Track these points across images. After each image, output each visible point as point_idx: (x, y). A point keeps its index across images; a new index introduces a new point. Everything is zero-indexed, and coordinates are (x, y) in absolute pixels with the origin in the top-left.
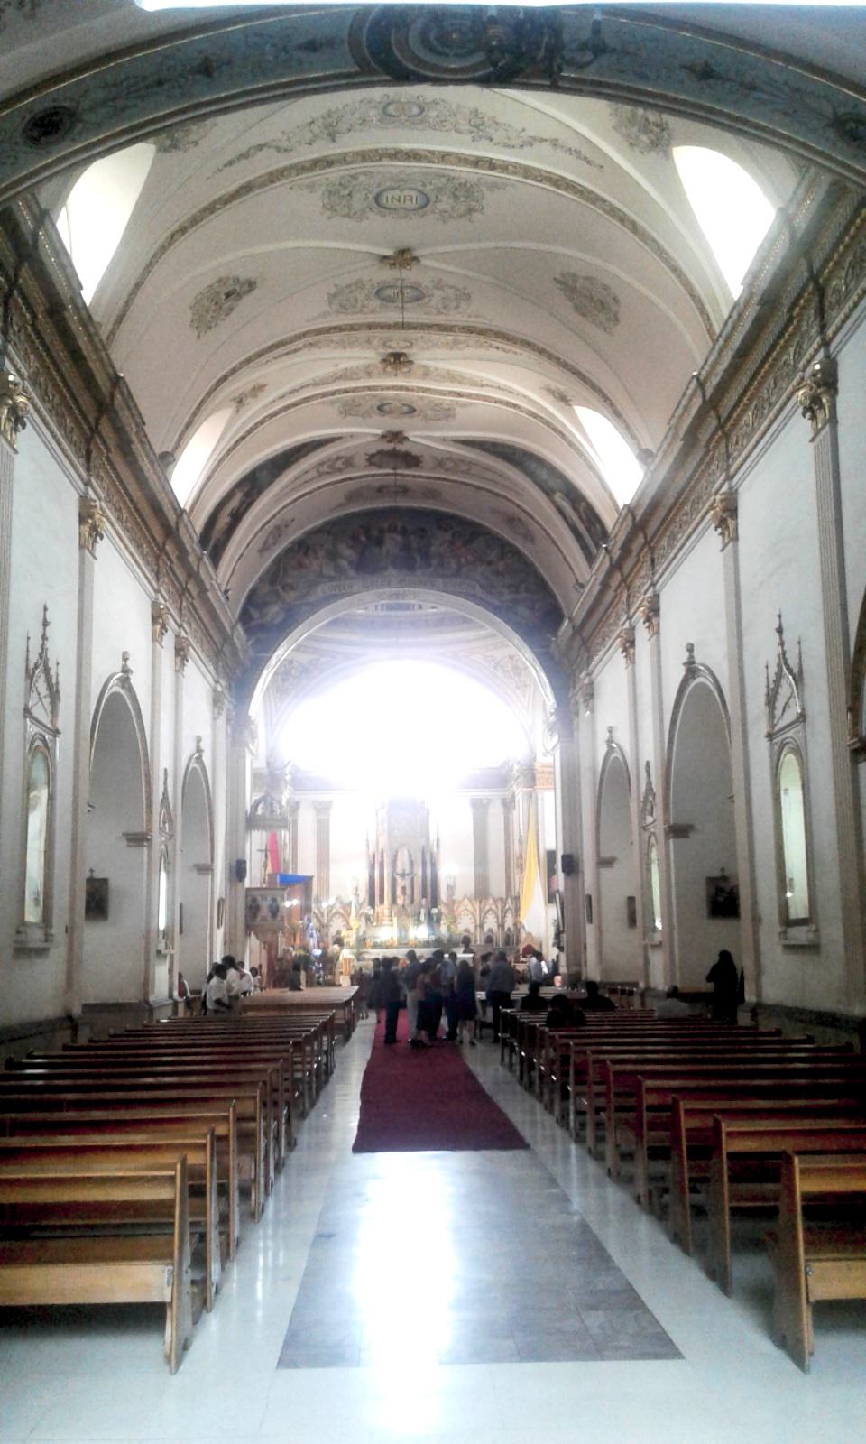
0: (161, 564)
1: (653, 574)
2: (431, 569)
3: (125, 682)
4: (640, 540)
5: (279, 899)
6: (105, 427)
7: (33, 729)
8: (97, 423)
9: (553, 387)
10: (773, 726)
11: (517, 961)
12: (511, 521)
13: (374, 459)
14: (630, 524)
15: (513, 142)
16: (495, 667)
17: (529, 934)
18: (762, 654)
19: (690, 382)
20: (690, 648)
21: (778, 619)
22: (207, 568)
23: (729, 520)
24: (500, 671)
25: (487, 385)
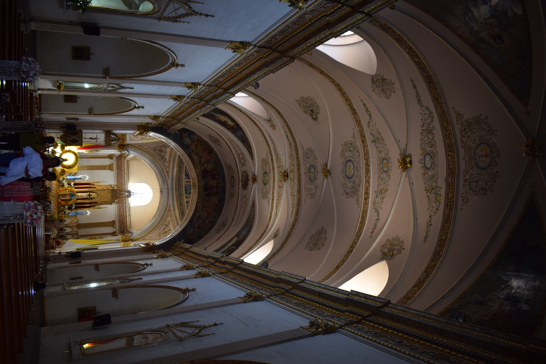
0: (214, 87)
3: (175, 65)
4: (230, 267)
5: (78, 143)
6: (276, 54)
8: (277, 51)
9: (279, 232)
12: (224, 224)
15: (376, 204)
16: (166, 225)
17: (65, 243)
18: (205, 318)
21: (220, 323)
22: (210, 108)
23: (252, 299)
24: (165, 227)
25: (277, 209)
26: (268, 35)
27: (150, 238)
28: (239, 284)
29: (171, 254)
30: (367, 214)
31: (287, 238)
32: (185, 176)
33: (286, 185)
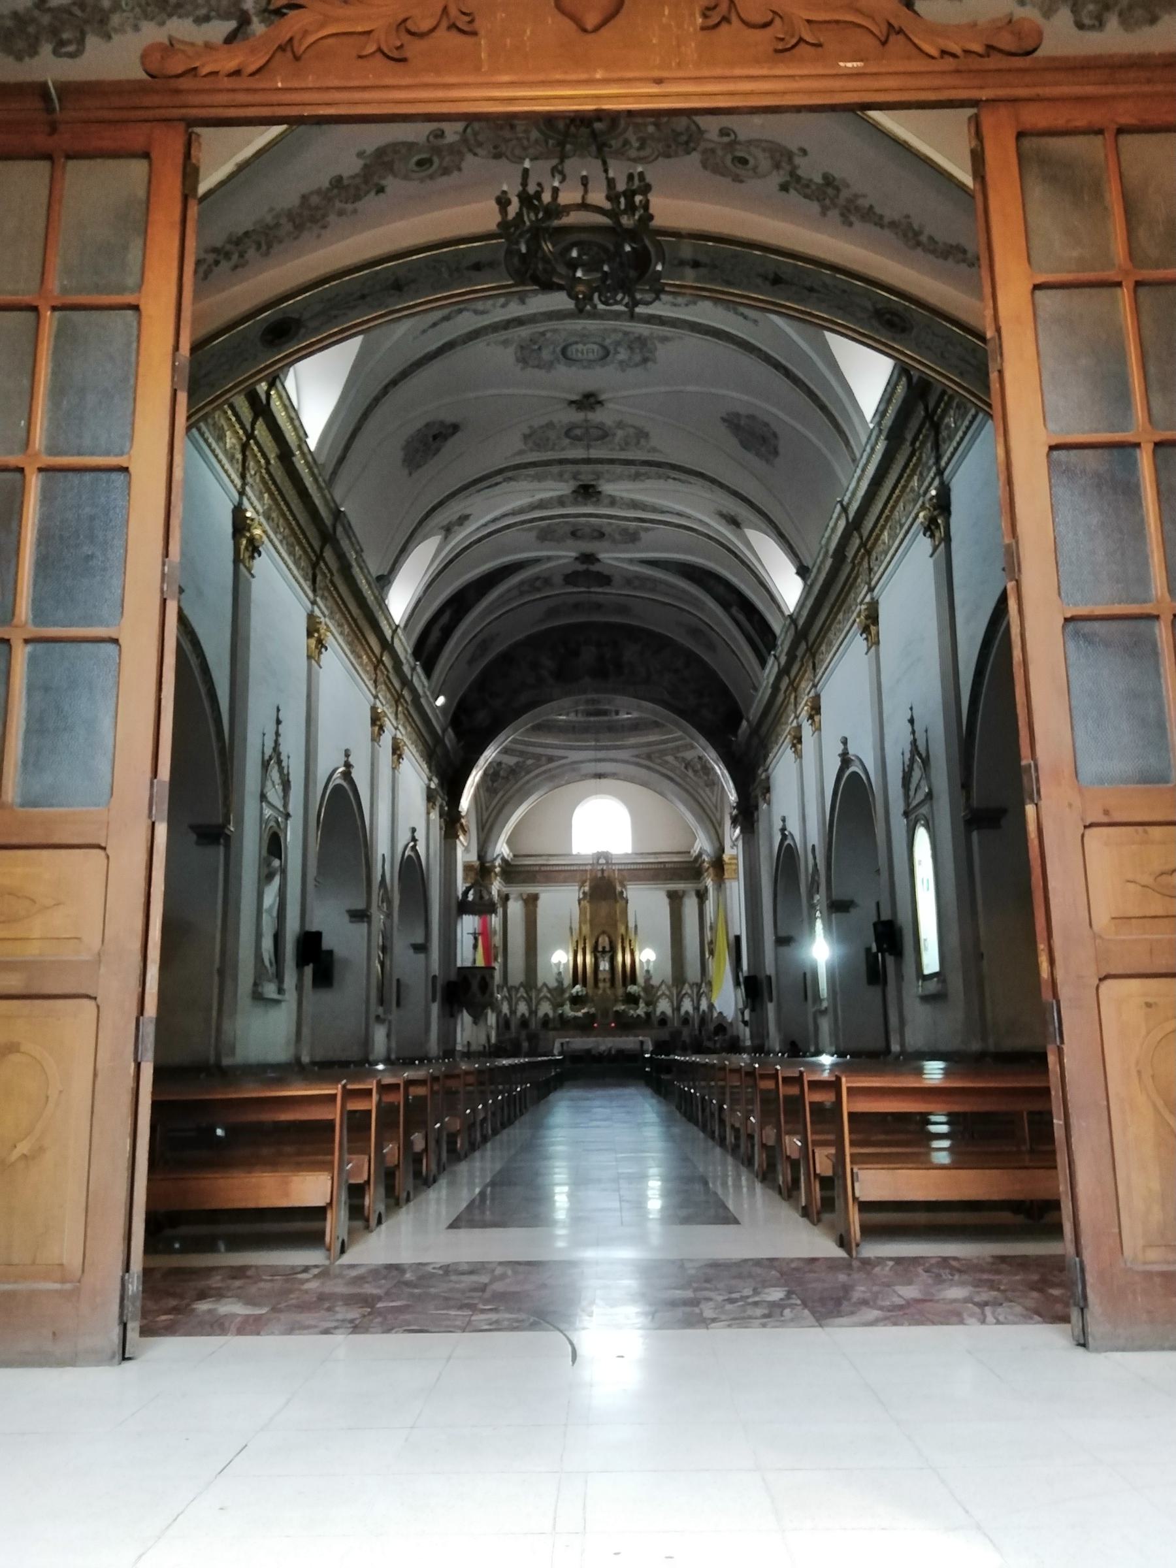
0: (378, 672)
4: (803, 646)
5: (488, 979)
6: (328, 554)
7: (268, 812)
8: (322, 551)
9: (725, 512)
10: (908, 804)
11: (709, 1039)
12: (695, 632)
13: (571, 578)
16: (686, 768)
17: (721, 1013)
20: (845, 741)
22: (419, 677)
23: (873, 628)
25: (668, 512)
30: (700, 324)
33: (608, 488)
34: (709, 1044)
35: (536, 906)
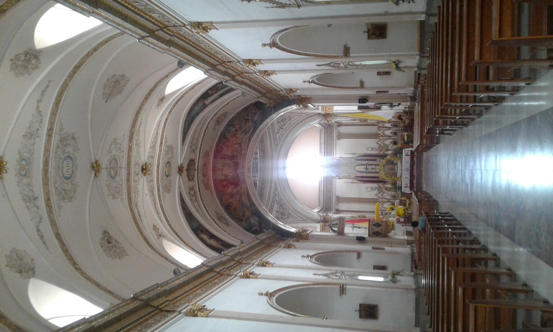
0: (224, 274)
1: (234, 62)
2: (238, 155)
3: (270, 295)
4: (220, 67)
5: (374, 223)
6: (155, 303)
8: (154, 307)
9: (156, 104)
11: (405, 122)
12: (218, 122)
13: (190, 178)
14: (212, 71)
16: (282, 129)
17: (393, 117)
19: (142, 43)
20: (264, 45)
23: (204, 26)
24: (284, 127)
25: (157, 131)
26: (165, 323)
27: (301, 115)
28: (213, 45)
29: (281, 92)
30: (52, 110)
31: (150, 94)
32: (257, 184)
34: (407, 121)
35: (342, 198)
